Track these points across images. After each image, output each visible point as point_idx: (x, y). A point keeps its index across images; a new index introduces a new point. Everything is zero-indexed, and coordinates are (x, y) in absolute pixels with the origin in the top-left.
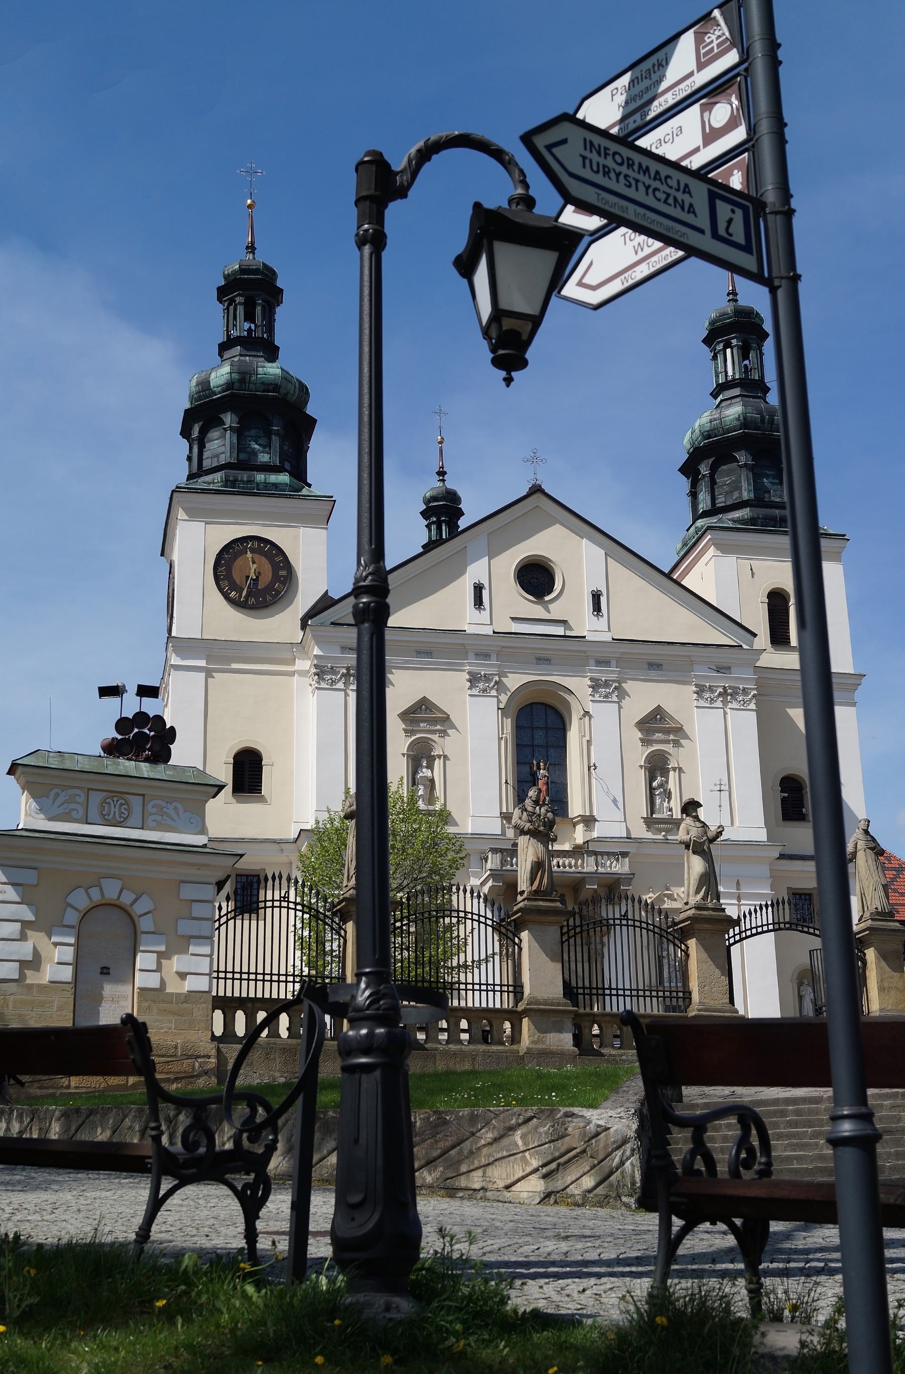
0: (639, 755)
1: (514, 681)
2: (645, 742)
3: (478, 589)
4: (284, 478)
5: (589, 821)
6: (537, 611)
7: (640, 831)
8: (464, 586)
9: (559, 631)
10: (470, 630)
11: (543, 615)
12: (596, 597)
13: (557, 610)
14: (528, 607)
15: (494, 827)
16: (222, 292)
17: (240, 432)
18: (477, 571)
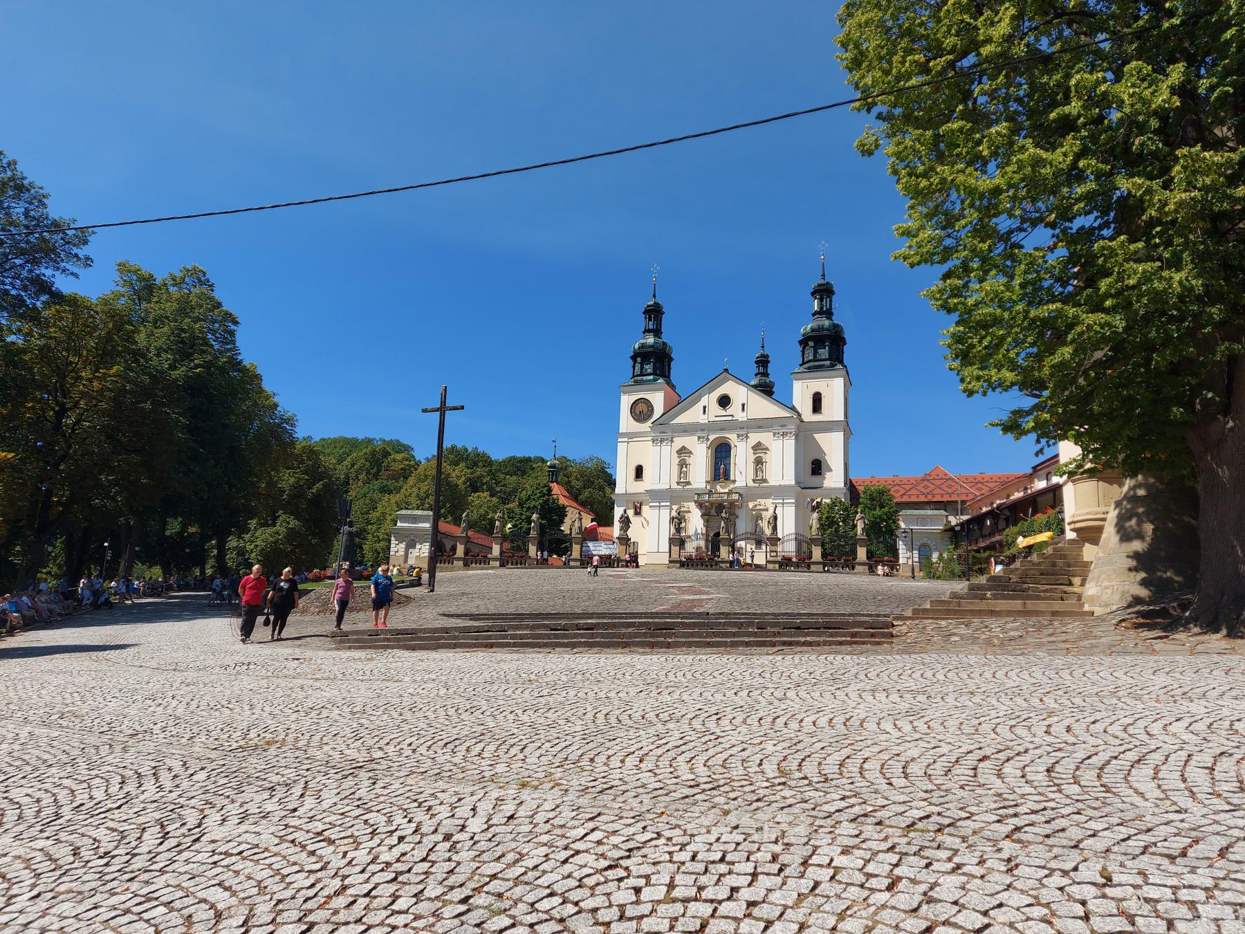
0: (752, 458)
1: (712, 437)
2: (755, 454)
3: (705, 407)
4: (651, 377)
5: (734, 481)
6: (724, 413)
7: (751, 484)
8: (699, 406)
9: (730, 418)
10: (701, 422)
11: (724, 413)
12: (743, 405)
13: (729, 412)
14: (721, 411)
15: (703, 485)
16: (644, 313)
17: (642, 364)
18: (704, 401)
